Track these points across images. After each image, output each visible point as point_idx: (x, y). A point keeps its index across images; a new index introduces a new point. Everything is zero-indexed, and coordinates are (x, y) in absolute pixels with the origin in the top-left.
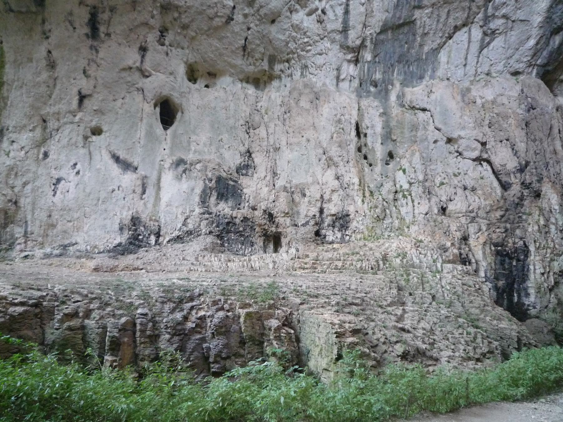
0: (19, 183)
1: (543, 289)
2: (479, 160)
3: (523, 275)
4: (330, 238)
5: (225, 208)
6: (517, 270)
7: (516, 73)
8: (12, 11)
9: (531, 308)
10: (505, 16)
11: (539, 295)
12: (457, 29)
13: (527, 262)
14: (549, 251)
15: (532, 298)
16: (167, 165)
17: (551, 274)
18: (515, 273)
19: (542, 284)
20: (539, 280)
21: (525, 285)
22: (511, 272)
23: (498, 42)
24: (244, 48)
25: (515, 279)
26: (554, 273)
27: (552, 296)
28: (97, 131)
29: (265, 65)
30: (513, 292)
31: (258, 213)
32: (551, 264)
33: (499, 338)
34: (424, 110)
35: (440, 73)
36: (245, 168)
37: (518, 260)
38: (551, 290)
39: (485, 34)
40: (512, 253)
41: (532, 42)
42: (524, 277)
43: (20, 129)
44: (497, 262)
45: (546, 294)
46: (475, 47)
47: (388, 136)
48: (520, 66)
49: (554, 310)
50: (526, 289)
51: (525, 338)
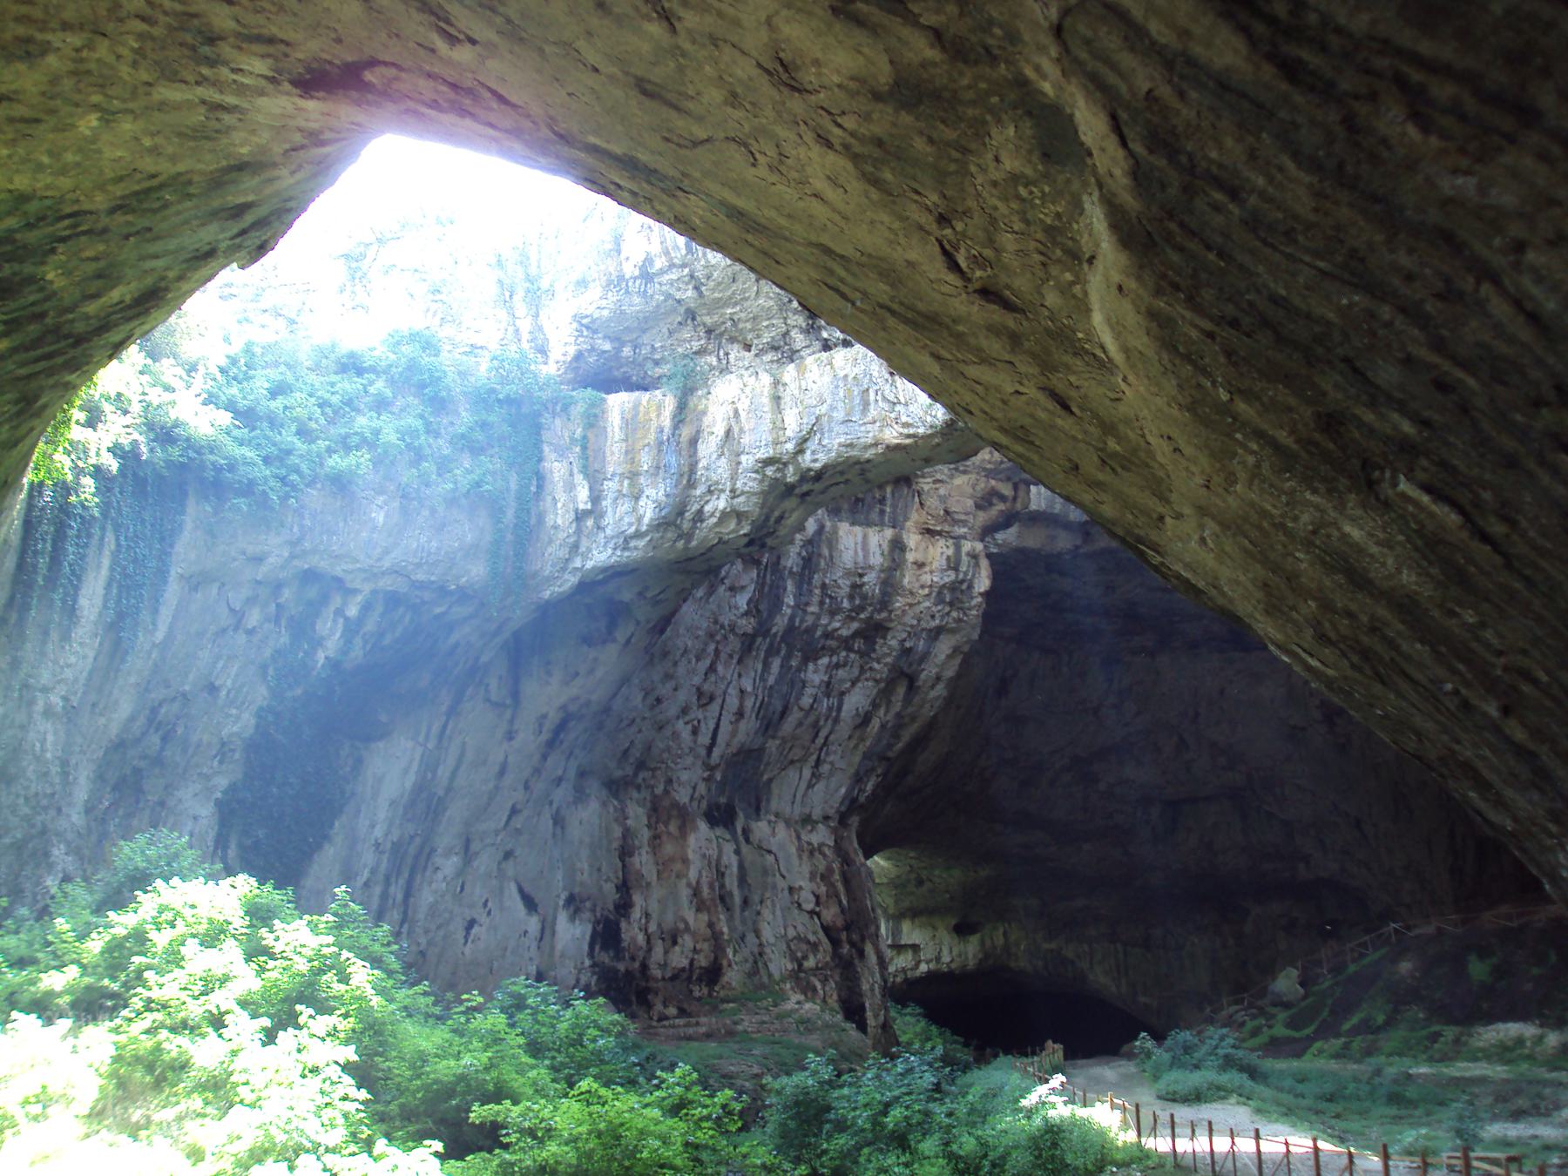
0: (433, 927)
2: (812, 913)
4: (697, 994)
5: (605, 958)
7: (826, 818)
8: (488, 700)
10: (832, 763)
12: (792, 762)
16: (561, 903)
23: (820, 786)
24: (626, 752)
28: (508, 855)
29: (629, 771)
31: (637, 965)
34: (770, 852)
35: (774, 805)
36: (624, 907)
39: (813, 775)
41: (843, 790)
43: (448, 853)
46: (803, 785)
47: (742, 880)
48: (831, 812)
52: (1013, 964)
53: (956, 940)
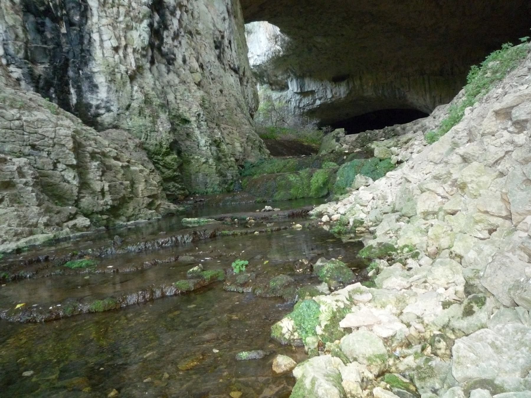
1: (119, 76)
3: (82, 51)
6: (70, 42)
9: (102, 111)
11: (112, 86)
13: (86, 28)
14: (122, 10)
15: (103, 93)
17: (130, 50)
18: (65, 48)
19: (116, 66)
20: (111, 60)
21: (87, 70)
22: (59, 45)
25: (67, 60)
26: (134, 51)
27: (136, 88)
30: (67, 84)
32: (128, 35)
33: (27, 150)
37: (70, 24)
38: (132, 78)
40: (55, 5)
42: (85, 56)
44: (29, 26)
45: (124, 83)
49: (141, 113)
50: (90, 77)
51: (92, 142)
52: (365, 95)
53: (334, 86)
